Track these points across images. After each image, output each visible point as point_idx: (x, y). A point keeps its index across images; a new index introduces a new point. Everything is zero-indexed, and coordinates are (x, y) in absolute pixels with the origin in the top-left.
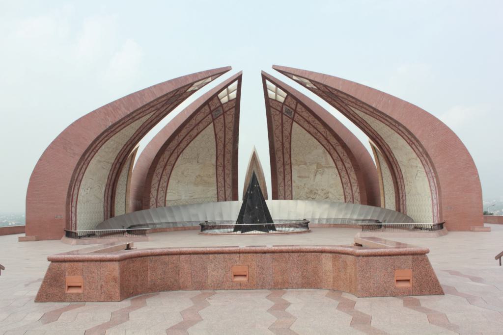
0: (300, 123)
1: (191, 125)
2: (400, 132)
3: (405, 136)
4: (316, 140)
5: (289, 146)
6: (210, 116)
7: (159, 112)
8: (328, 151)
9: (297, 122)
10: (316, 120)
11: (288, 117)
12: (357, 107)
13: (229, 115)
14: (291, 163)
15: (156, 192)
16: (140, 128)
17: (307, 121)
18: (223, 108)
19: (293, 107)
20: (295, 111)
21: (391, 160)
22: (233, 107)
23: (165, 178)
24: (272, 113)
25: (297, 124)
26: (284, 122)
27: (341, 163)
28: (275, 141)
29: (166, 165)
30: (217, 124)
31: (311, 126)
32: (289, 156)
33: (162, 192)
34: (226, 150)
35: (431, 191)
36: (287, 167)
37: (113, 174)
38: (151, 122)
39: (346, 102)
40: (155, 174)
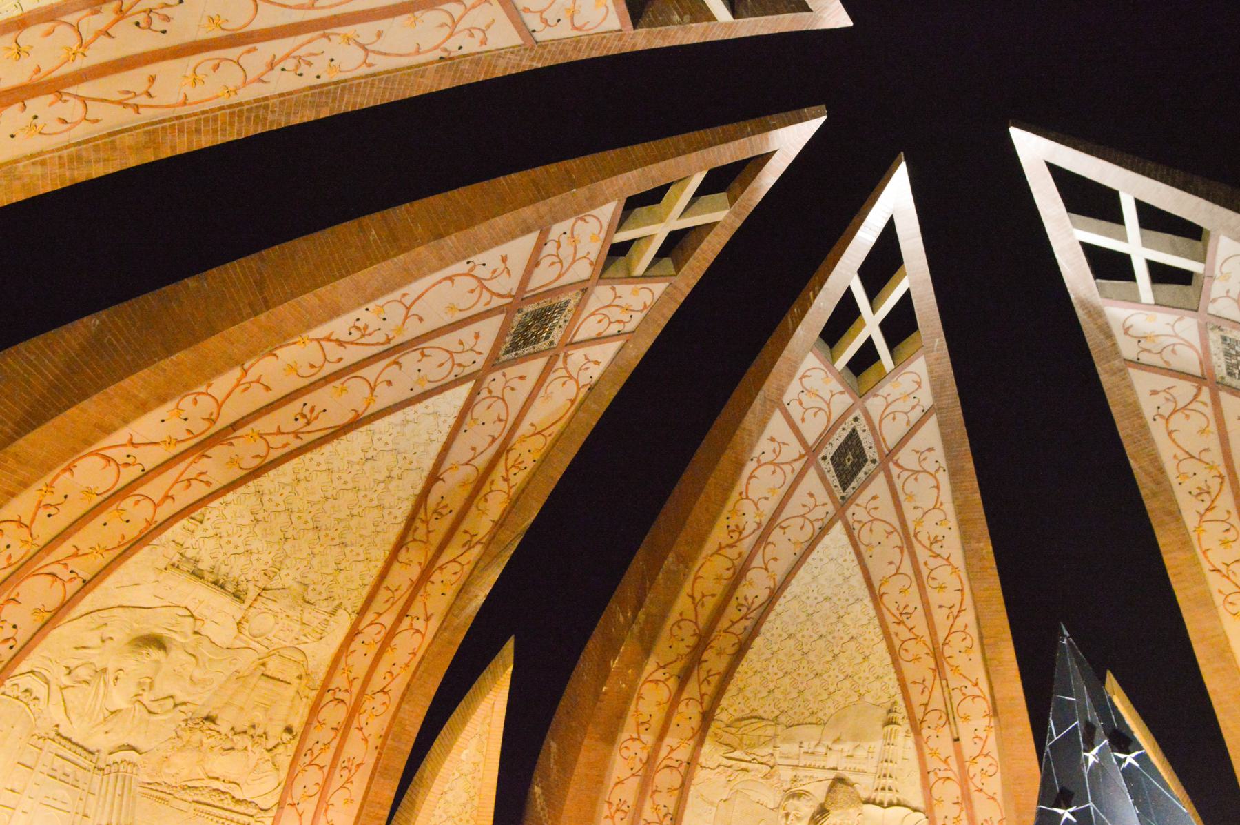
0: (865, 537)
1: (364, 331)
4: (883, 646)
6: (490, 328)
8: (911, 717)
9: (849, 530)
11: (830, 493)
13: (570, 377)
18: (580, 306)
19: (892, 432)
24: (763, 446)
25: (845, 539)
26: (783, 516)
27: (958, 792)
28: (673, 617)
30: (479, 410)
31: (907, 567)
32: (696, 721)
36: (666, 779)
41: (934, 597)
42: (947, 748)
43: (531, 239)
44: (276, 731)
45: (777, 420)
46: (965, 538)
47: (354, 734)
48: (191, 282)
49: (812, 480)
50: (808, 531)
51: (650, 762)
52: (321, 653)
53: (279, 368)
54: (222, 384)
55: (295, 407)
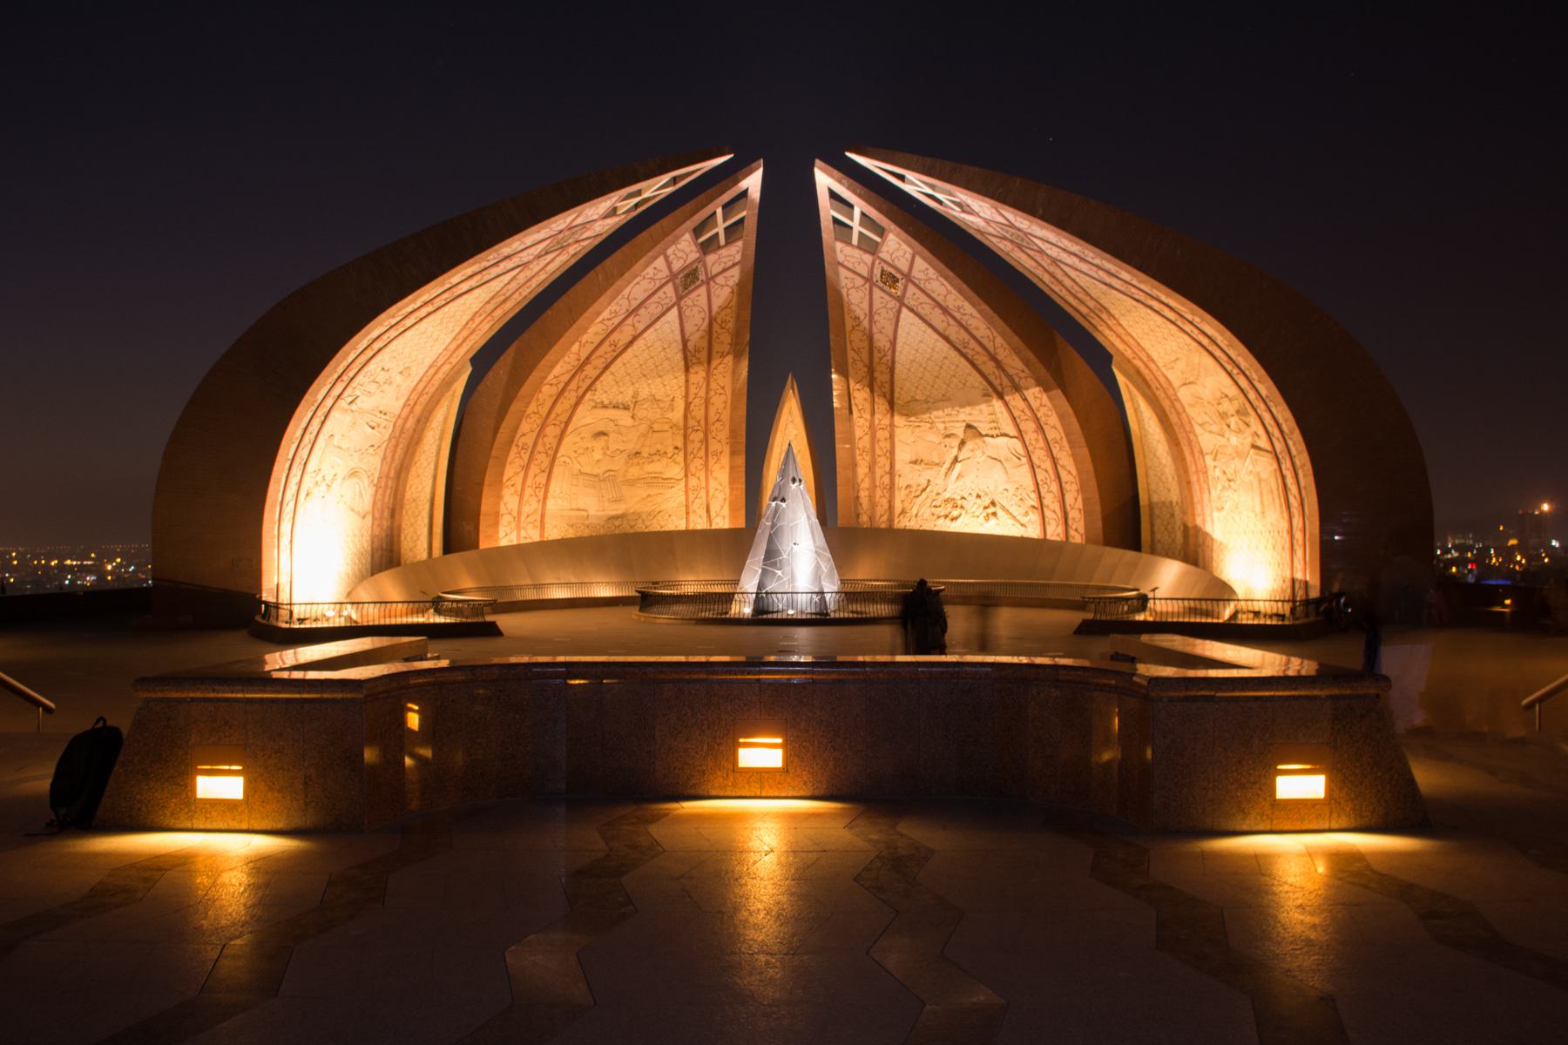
0: (920, 311)
2: (1205, 341)
3: (1218, 353)
5: (886, 378)
6: (669, 289)
7: (528, 273)
9: (912, 310)
10: (967, 305)
11: (890, 295)
12: (1084, 267)
14: (892, 425)
15: (517, 499)
16: (472, 319)
17: (940, 306)
19: (904, 266)
20: (908, 277)
21: (1173, 418)
22: (734, 265)
23: (542, 460)
24: (843, 282)
28: (850, 361)
29: (543, 427)
32: (886, 406)
33: (533, 501)
34: (713, 386)
35: (1288, 507)
37: (396, 446)
38: (504, 301)
39: (1053, 252)
40: (514, 450)
41: (978, 334)
42: (1022, 405)
43: (661, 259)
44: (670, 451)
45: (842, 271)
46: (974, 305)
47: (711, 441)
48: (549, 312)
49: (877, 293)
50: (891, 314)
51: (872, 426)
52: (677, 415)
53: (594, 332)
54: (575, 348)
55: (607, 343)
